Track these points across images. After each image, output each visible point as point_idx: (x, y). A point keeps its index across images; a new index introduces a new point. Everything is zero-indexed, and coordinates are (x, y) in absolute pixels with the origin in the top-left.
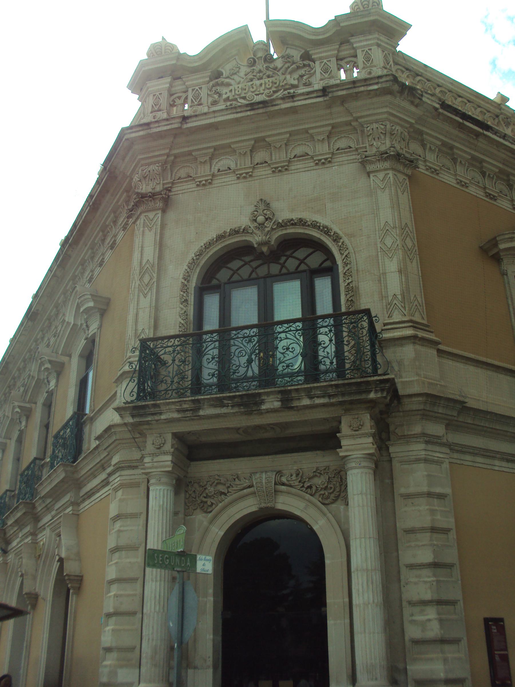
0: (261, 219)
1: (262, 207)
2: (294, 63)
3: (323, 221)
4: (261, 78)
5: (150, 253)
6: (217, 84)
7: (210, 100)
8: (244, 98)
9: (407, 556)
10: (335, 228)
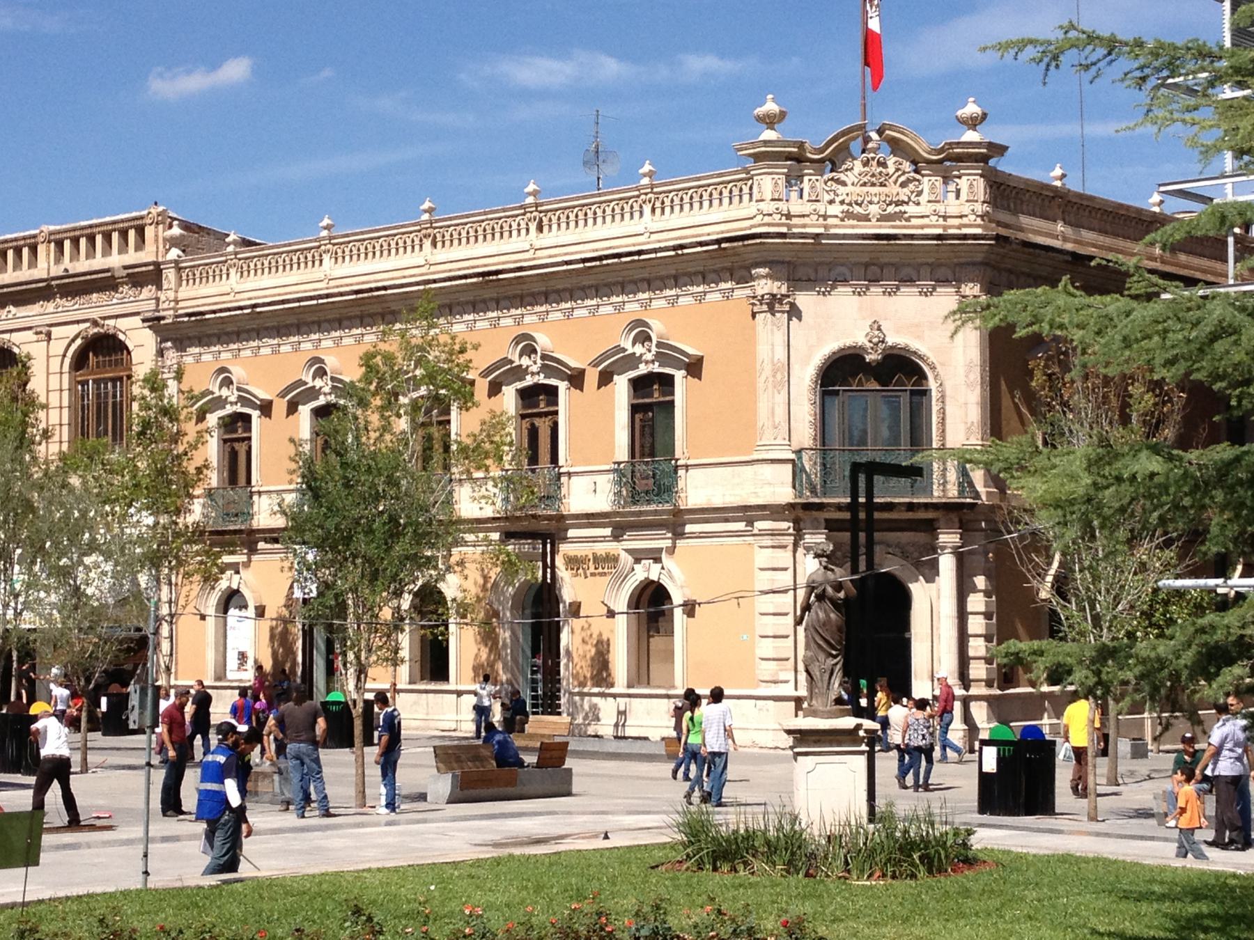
0: (875, 340)
1: (876, 326)
2: (904, 173)
3: (923, 350)
4: (873, 185)
5: (781, 354)
6: (832, 179)
7: (827, 197)
8: (860, 205)
9: (970, 607)
10: (932, 358)
